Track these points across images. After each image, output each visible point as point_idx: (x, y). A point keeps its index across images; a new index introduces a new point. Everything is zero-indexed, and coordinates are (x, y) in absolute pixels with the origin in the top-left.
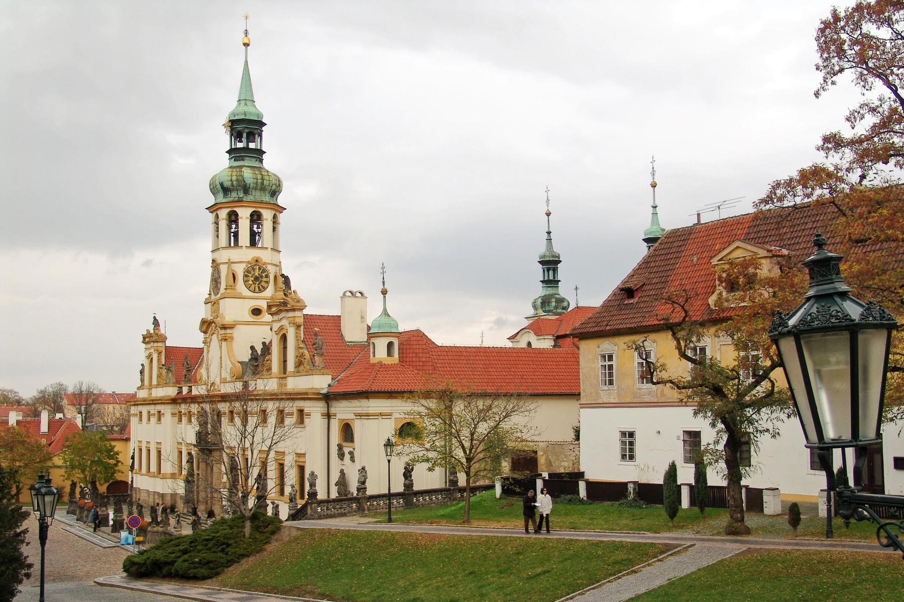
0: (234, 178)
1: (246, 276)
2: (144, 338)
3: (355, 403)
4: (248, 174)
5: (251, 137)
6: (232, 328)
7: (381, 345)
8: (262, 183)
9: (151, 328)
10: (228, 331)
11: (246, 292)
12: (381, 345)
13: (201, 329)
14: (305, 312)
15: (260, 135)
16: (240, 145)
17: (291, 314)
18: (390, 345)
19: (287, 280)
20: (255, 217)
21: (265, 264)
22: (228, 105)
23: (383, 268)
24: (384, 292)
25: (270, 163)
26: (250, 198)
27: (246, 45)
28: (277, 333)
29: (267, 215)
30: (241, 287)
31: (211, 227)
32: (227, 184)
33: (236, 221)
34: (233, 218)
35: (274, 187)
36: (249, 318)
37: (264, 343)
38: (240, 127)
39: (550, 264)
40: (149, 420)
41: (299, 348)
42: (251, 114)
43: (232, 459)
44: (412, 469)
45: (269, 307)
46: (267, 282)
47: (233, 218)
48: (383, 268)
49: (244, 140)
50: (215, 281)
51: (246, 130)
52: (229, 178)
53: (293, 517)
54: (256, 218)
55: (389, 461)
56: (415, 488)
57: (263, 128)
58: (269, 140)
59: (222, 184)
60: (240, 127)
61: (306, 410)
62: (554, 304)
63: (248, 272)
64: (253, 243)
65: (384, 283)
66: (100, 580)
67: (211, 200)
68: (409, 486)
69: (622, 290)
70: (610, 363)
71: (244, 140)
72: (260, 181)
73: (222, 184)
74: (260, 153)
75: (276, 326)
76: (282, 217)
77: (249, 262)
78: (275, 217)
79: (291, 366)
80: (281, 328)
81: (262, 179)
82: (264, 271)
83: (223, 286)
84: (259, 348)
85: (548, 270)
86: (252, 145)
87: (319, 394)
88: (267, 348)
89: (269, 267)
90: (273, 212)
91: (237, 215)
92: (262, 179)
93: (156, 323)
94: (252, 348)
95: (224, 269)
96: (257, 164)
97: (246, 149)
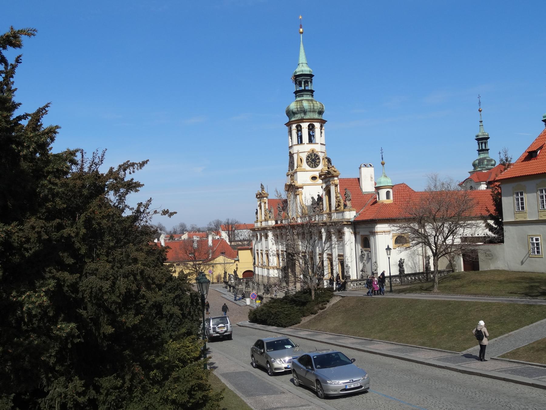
0: (298, 107)
1: (307, 159)
2: (257, 196)
3: (369, 225)
4: (306, 104)
5: (306, 82)
6: (302, 188)
7: (383, 192)
8: (314, 108)
9: (260, 190)
10: (300, 190)
11: (308, 168)
12: (383, 192)
15: (311, 82)
16: (301, 89)
18: (388, 193)
19: (329, 161)
20: (311, 127)
23: (382, 150)
24: (383, 164)
28: (325, 190)
29: (317, 125)
30: (305, 165)
32: (295, 110)
33: (301, 130)
34: (299, 129)
35: (320, 110)
36: (310, 181)
37: (318, 195)
39: (482, 140)
40: (261, 239)
41: (337, 197)
42: (305, 71)
44: (404, 262)
45: (320, 176)
46: (319, 162)
47: (299, 129)
48: (382, 150)
49: (303, 85)
53: (339, 289)
54: (311, 128)
55: (389, 258)
56: (406, 272)
57: (313, 78)
62: (486, 163)
63: (308, 157)
64: (310, 141)
65: (382, 158)
66: (240, 323)
67: (287, 120)
68: (401, 270)
69: (529, 152)
70: (522, 197)
71: (303, 85)
72: (312, 107)
77: (308, 152)
78: (321, 126)
79: (333, 208)
82: (317, 156)
84: (316, 198)
85: (482, 143)
86: (307, 88)
87: (349, 222)
88: (320, 198)
89: (320, 154)
91: (301, 126)
94: (312, 198)
95: (295, 156)
96: (310, 98)
97: (305, 90)
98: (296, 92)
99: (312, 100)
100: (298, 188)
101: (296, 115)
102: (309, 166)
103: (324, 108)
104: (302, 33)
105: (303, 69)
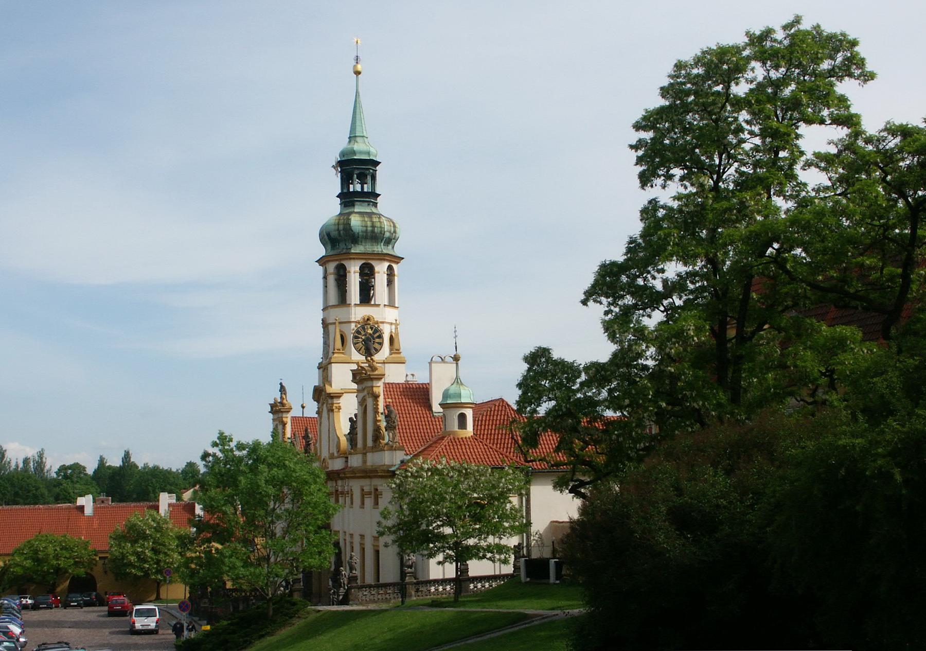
0: (341, 227)
1: (355, 337)
4: (356, 222)
5: (362, 178)
8: (373, 231)
10: (335, 401)
13: (314, 398)
15: (374, 178)
17: (369, 384)
21: (377, 323)
22: (337, 146)
25: (384, 206)
27: (357, 73)
29: (381, 268)
31: (321, 281)
32: (334, 234)
33: (345, 276)
35: (387, 235)
42: (361, 153)
43: (337, 544)
46: (381, 344)
47: (342, 273)
50: (326, 344)
51: (356, 171)
58: (384, 182)
59: (328, 235)
61: (379, 488)
63: (358, 332)
67: (321, 251)
72: (369, 229)
73: (328, 235)
75: (361, 395)
78: (390, 268)
81: (373, 227)
82: (376, 331)
83: (331, 350)
89: (382, 326)
90: (386, 264)
92: (373, 227)
93: (282, 389)
95: (331, 328)
97: (362, 194)
99: (370, 215)
100: (332, 398)
102: (359, 351)
103: (398, 230)
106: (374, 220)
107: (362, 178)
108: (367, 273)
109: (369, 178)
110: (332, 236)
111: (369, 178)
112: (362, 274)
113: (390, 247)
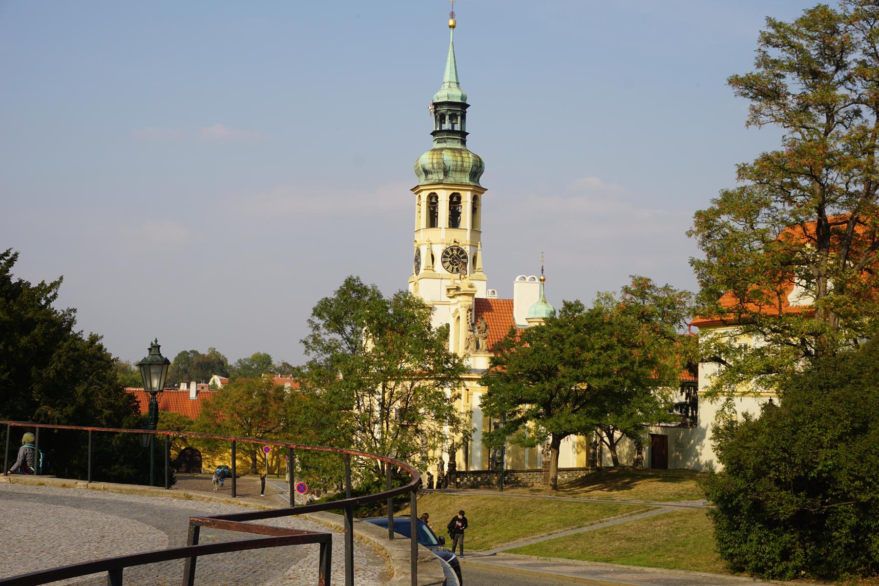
0: (435, 161)
4: (448, 157)
8: (462, 165)
14: (476, 296)
15: (463, 117)
20: (455, 199)
26: (450, 180)
29: (467, 198)
32: (428, 167)
36: (445, 298)
38: (443, 109)
42: (453, 96)
46: (465, 264)
47: (434, 201)
52: (430, 161)
60: (443, 109)
71: (447, 122)
72: (459, 163)
74: (463, 134)
75: (453, 309)
76: (484, 198)
80: (457, 311)
81: (462, 161)
82: (462, 252)
86: (457, 127)
91: (437, 197)
92: (462, 161)
96: (459, 146)
97: (452, 132)
98: (434, 134)
101: (430, 176)
104: (453, 27)
105: (450, 92)
106: (464, 155)
107: (453, 117)
108: (455, 202)
109: (459, 118)
110: (427, 168)
111: (459, 118)
112: (451, 202)
113: (476, 179)
